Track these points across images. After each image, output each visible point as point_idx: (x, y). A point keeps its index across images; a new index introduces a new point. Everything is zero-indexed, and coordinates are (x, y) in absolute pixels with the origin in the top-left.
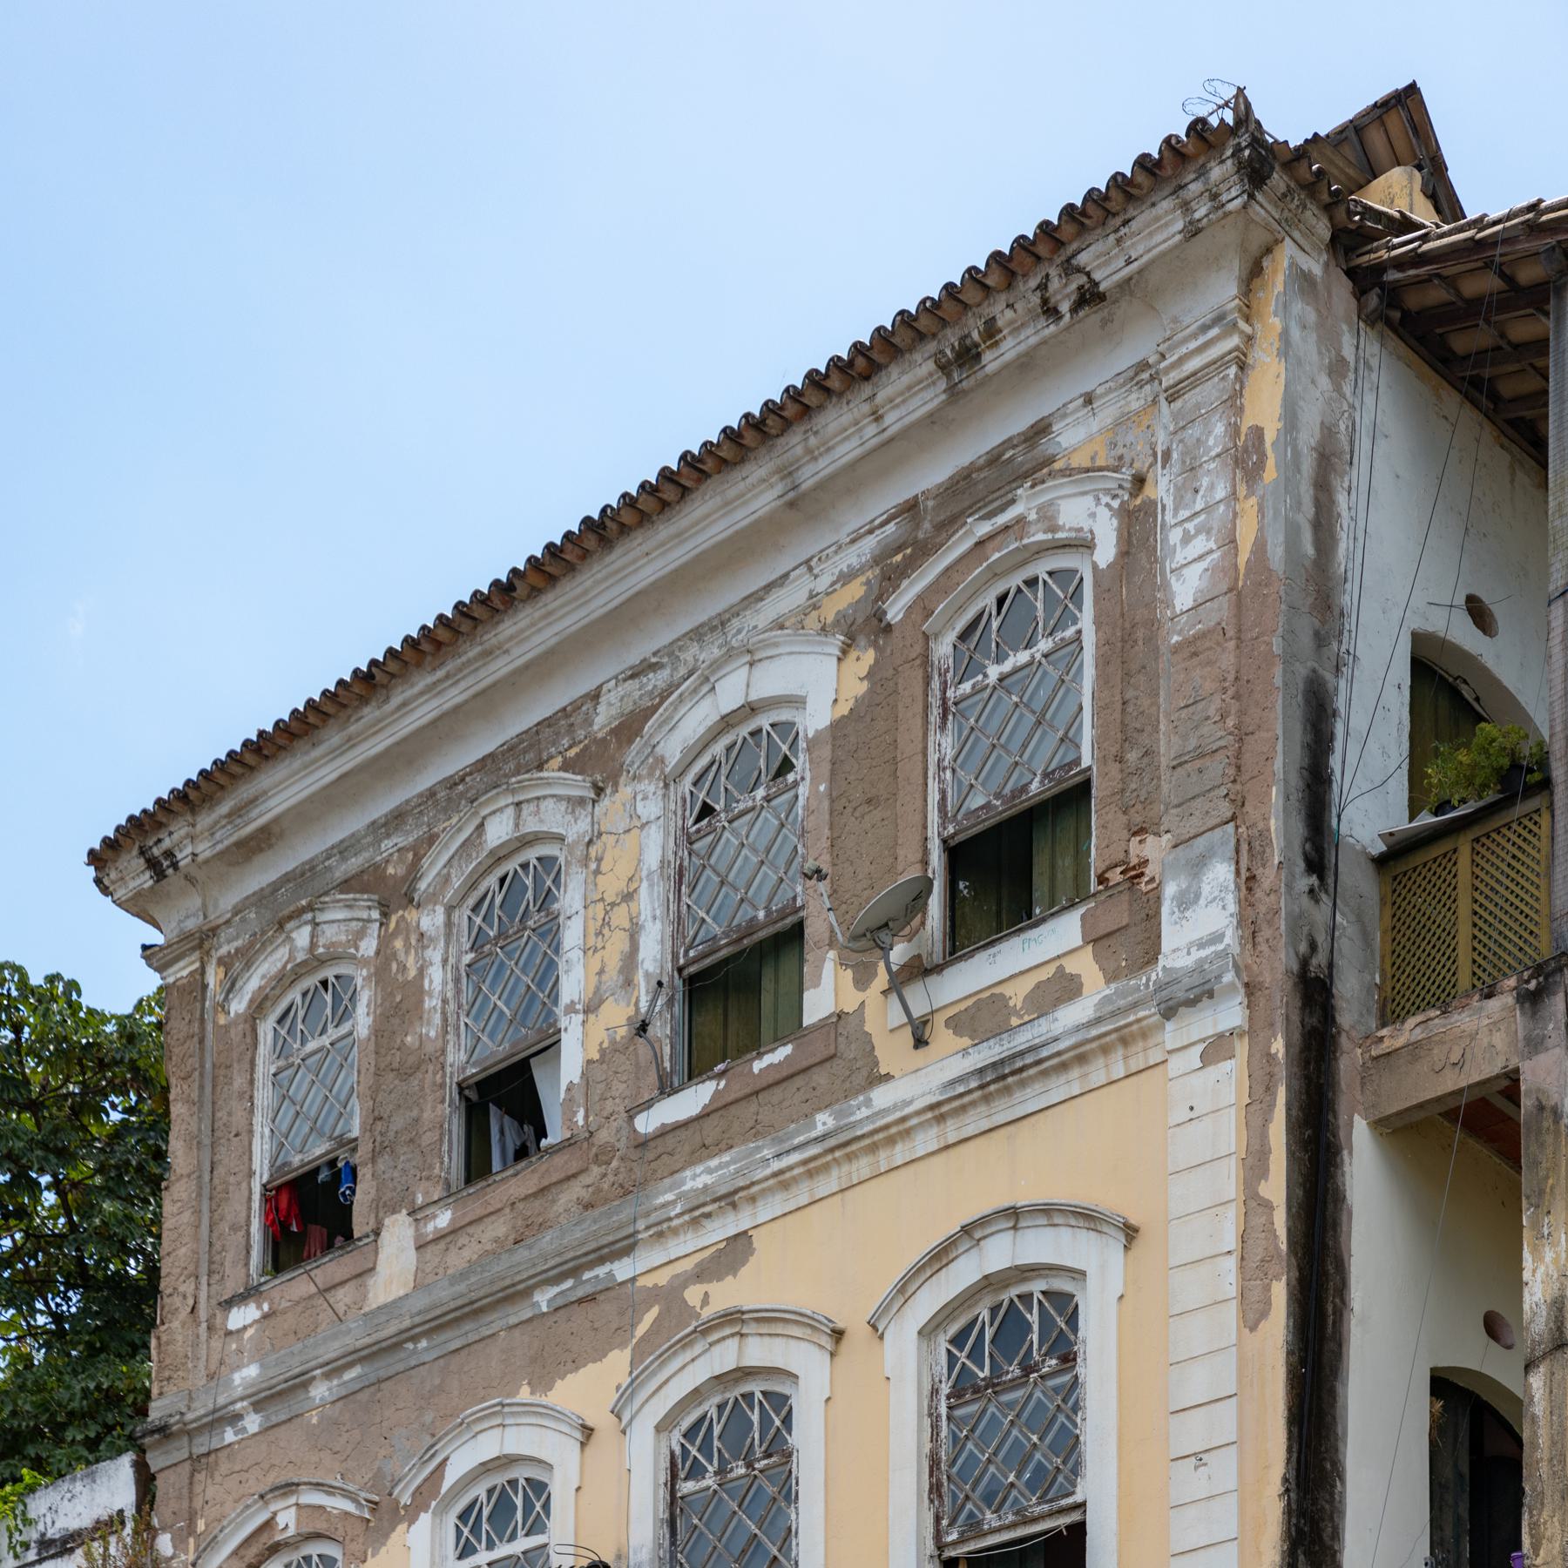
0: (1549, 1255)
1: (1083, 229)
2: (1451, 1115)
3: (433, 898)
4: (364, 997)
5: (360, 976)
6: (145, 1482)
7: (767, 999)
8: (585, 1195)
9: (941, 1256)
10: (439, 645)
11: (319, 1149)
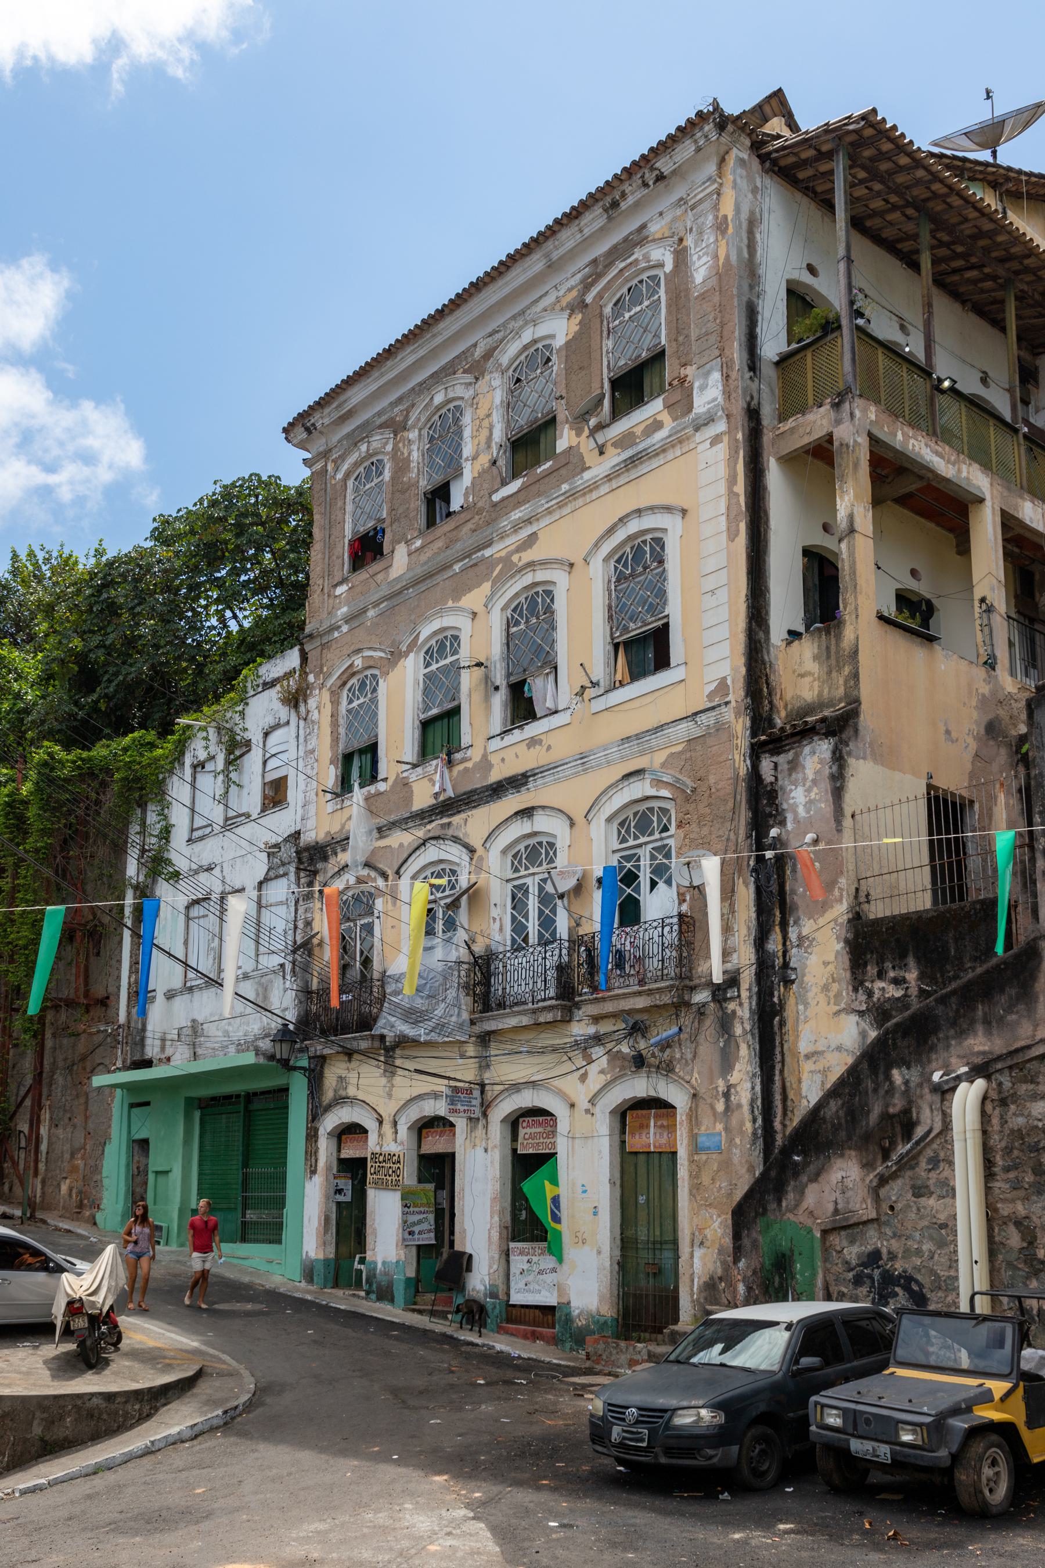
0: (846, 498)
1: (657, 154)
2: (807, 452)
3: (414, 426)
4: (388, 466)
5: (386, 459)
6: (304, 658)
7: (542, 446)
8: (473, 527)
9: (611, 531)
10: (415, 335)
11: (370, 524)
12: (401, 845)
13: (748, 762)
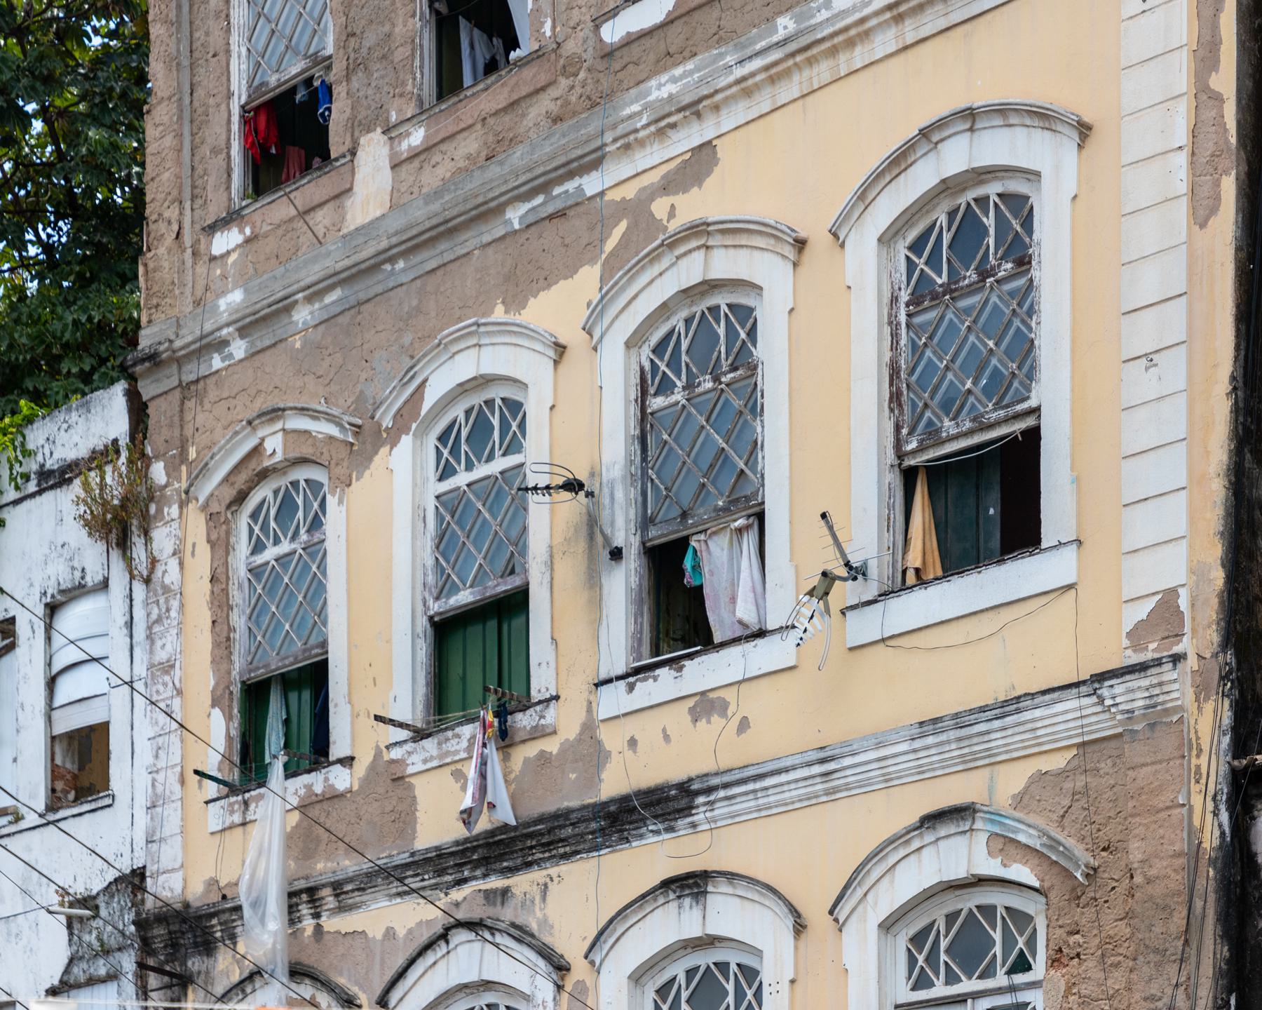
12: (390, 933)
13: (1225, 817)
